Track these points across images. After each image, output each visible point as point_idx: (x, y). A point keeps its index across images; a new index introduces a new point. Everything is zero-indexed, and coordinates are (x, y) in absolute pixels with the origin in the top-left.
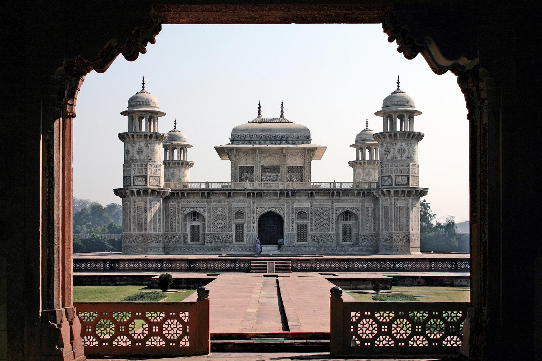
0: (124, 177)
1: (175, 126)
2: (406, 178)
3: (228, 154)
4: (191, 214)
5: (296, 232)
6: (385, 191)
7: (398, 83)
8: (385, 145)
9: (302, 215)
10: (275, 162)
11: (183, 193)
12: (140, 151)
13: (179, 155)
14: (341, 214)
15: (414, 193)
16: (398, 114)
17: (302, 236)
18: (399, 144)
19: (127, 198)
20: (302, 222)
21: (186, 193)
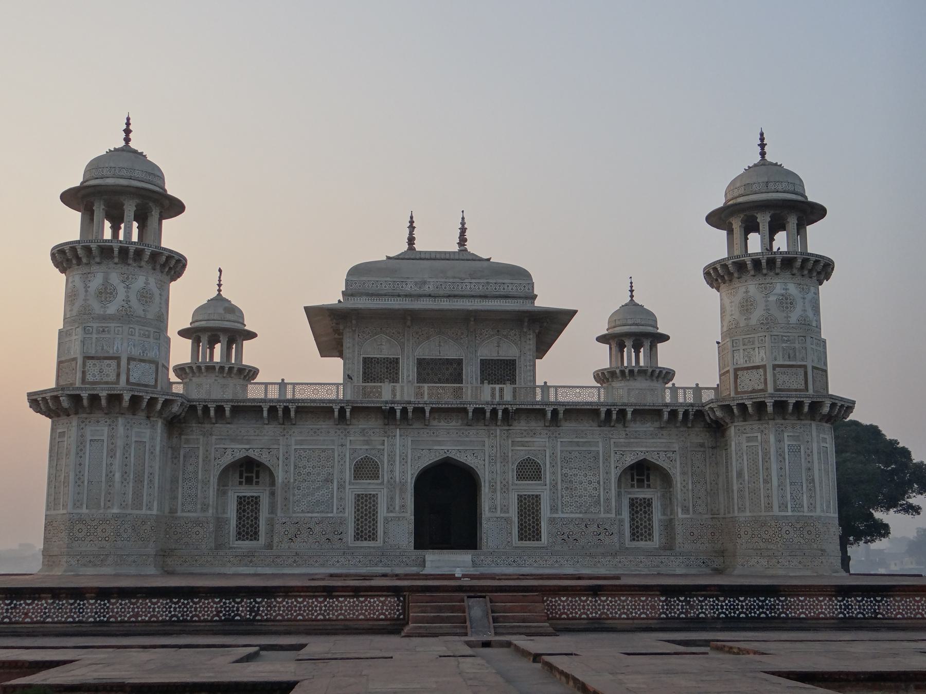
0: (60, 363)
1: (219, 291)
2: (801, 371)
3: (337, 331)
4: (241, 466)
5: (513, 514)
6: (748, 403)
7: (762, 146)
8: (744, 290)
9: (529, 470)
10: (450, 351)
11: (220, 410)
12: (106, 293)
13: (227, 353)
14: (625, 471)
15: (826, 410)
16: (772, 212)
17: (529, 527)
18: (779, 289)
19: (64, 419)
20: (530, 487)
21: (227, 409)
